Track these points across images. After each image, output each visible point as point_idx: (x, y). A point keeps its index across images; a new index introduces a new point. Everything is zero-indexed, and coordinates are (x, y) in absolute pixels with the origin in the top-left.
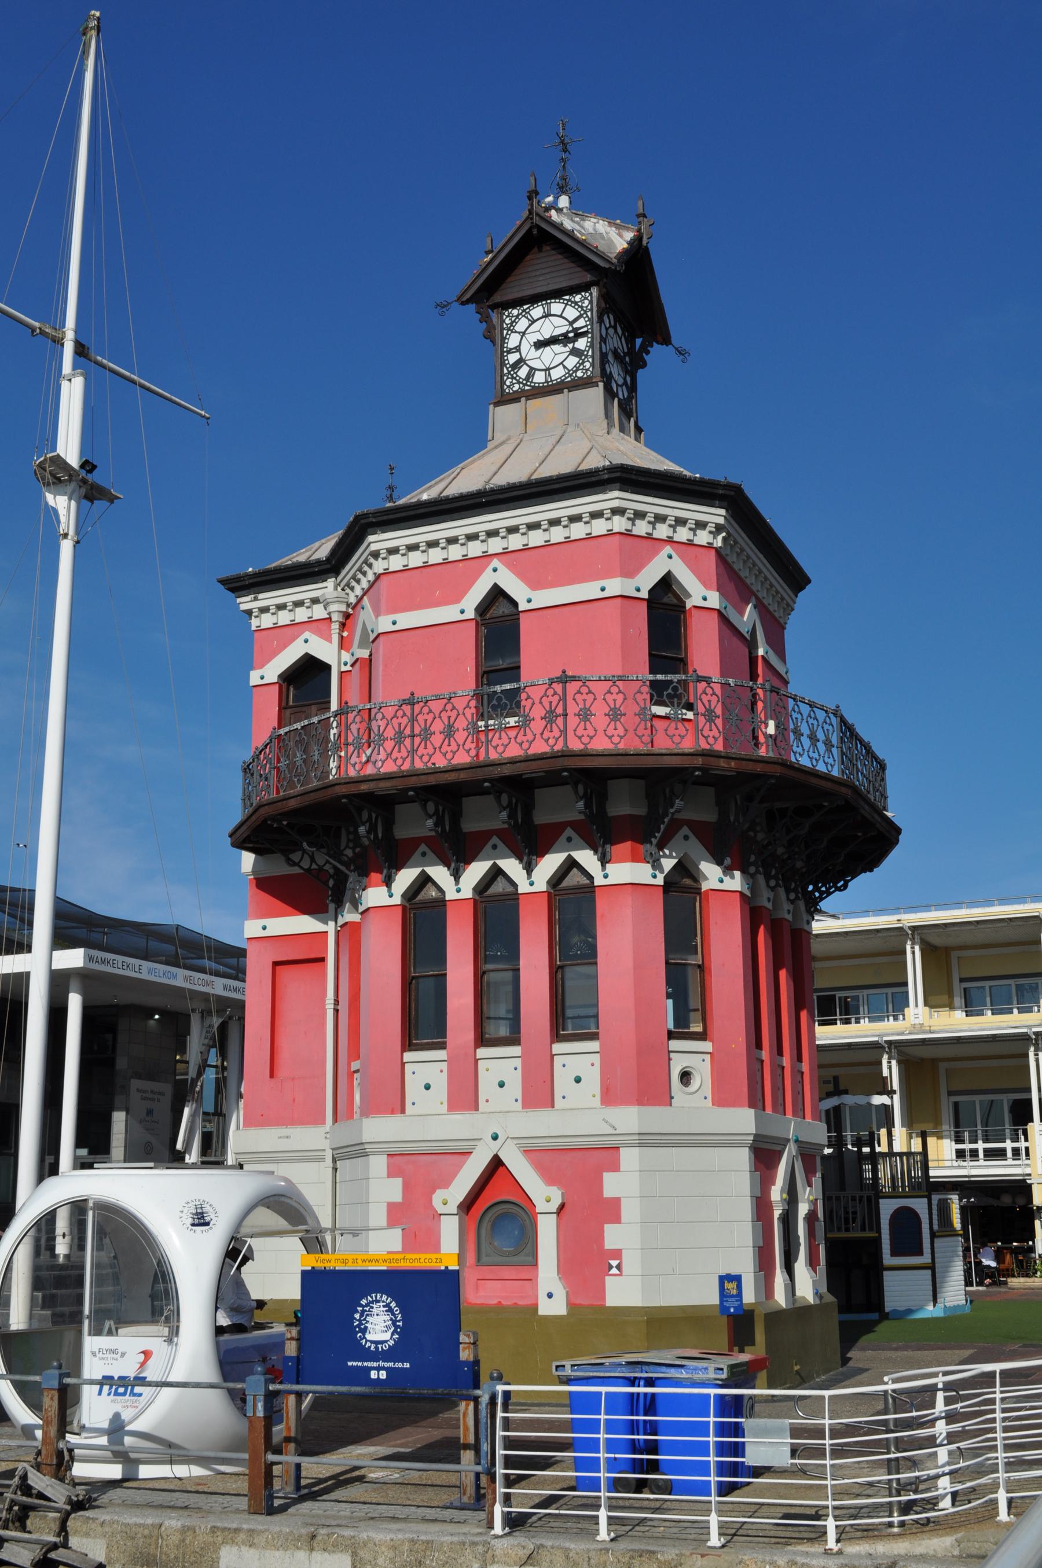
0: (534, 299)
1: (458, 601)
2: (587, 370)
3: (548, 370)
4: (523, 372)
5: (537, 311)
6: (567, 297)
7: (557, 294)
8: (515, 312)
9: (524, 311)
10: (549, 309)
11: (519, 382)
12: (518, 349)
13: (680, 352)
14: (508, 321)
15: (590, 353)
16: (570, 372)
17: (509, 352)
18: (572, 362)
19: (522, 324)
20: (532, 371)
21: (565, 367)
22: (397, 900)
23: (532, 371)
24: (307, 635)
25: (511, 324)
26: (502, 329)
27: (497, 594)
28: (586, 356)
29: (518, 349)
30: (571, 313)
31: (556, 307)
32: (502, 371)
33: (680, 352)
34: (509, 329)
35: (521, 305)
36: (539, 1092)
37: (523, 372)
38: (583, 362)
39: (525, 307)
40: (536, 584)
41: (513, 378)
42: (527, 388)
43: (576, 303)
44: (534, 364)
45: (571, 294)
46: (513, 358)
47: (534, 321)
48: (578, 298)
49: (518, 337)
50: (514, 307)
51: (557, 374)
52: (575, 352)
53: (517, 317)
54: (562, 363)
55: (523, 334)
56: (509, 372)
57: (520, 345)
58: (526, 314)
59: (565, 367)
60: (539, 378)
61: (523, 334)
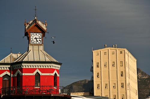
0: (35, 33)
4: (33, 42)
5: (35, 34)
7: (38, 33)
13: (46, 38)
18: (39, 42)
19: (33, 35)
24: (6, 71)
27: (37, 72)
30: (39, 35)
31: (37, 34)
33: (46, 38)
44: (35, 41)
51: (37, 43)
52: (40, 40)
60: (35, 43)
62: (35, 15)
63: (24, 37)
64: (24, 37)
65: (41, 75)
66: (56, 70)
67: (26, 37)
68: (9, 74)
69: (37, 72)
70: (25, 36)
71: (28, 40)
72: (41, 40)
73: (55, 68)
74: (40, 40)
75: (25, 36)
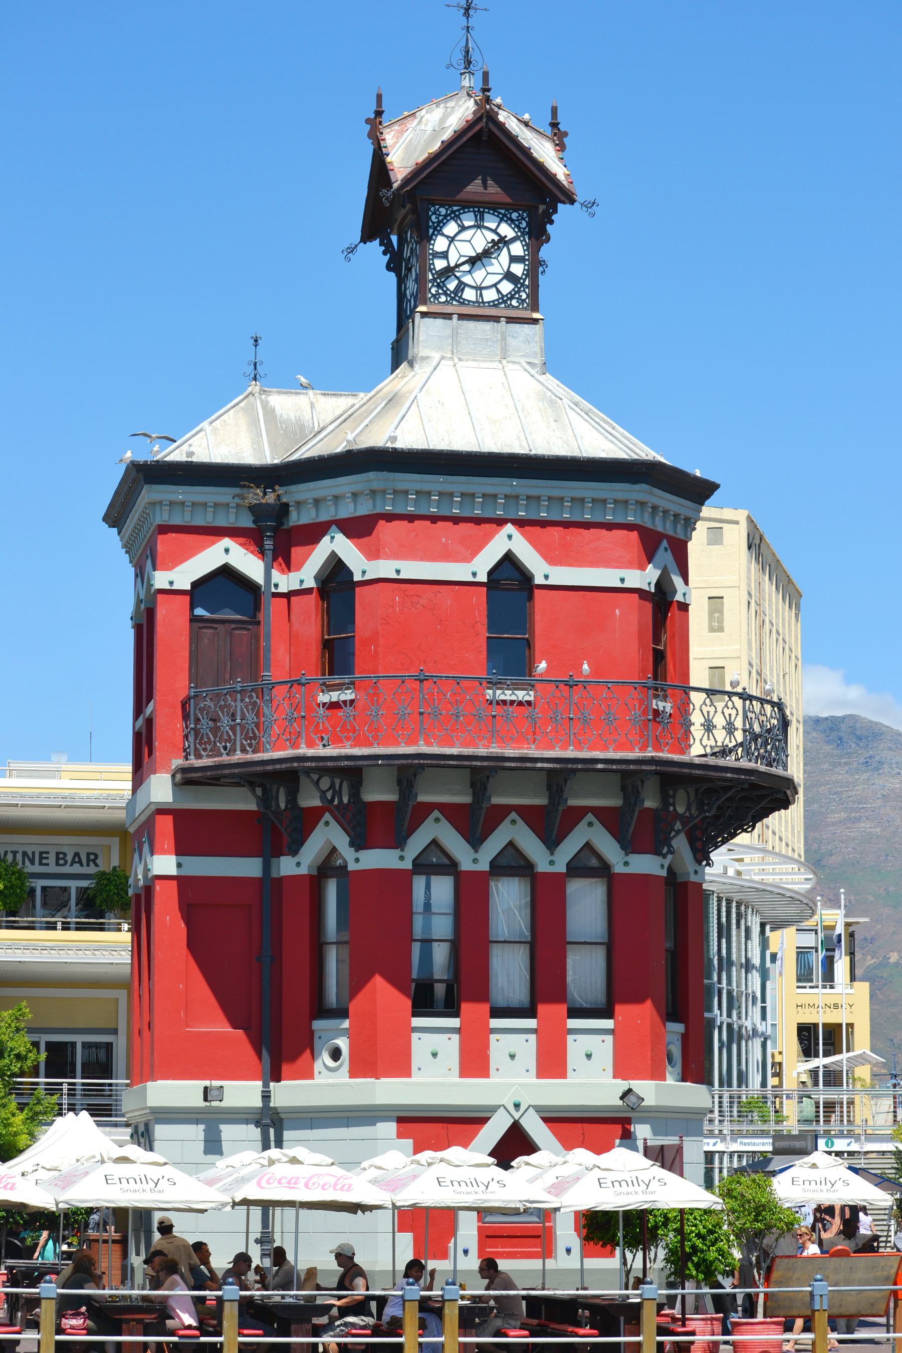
1: (468, 559)
2: (524, 301)
3: (479, 289)
4: (452, 285)
5: (468, 220)
6: (503, 211)
8: (443, 211)
9: (453, 212)
10: (482, 219)
11: (445, 294)
12: (445, 255)
14: (433, 218)
15: (527, 283)
16: (504, 299)
17: (437, 255)
18: (507, 287)
19: (451, 228)
20: (461, 286)
21: (498, 291)
22: (408, 865)
23: (461, 286)
24: (227, 542)
25: (439, 222)
26: (428, 227)
27: (509, 559)
28: (523, 285)
29: (445, 255)
30: (506, 230)
32: (425, 276)
34: (435, 229)
35: (451, 206)
36: (552, 1063)
37: (452, 285)
38: (518, 292)
39: (455, 208)
40: (552, 559)
41: (438, 286)
42: (454, 303)
43: (512, 221)
44: (467, 279)
45: (507, 210)
46: (440, 264)
47: (463, 228)
48: (514, 215)
49: (446, 242)
50: (442, 206)
51: (490, 295)
52: (509, 276)
53: (446, 216)
54: (495, 285)
55: (452, 240)
56: (434, 279)
57: (447, 252)
58: (456, 217)
59: (498, 291)
61: (452, 240)
62: (459, 56)
63: (352, 250)
64: (352, 250)
65: (539, 580)
66: (665, 543)
67: (375, 247)
68: (251, 566)
69: (509, 559)
70: (367, 236)
71: (392, 277)
72: (518, 269)
73: (660, 528)
74: (509, 276)
75: (367, 236)
